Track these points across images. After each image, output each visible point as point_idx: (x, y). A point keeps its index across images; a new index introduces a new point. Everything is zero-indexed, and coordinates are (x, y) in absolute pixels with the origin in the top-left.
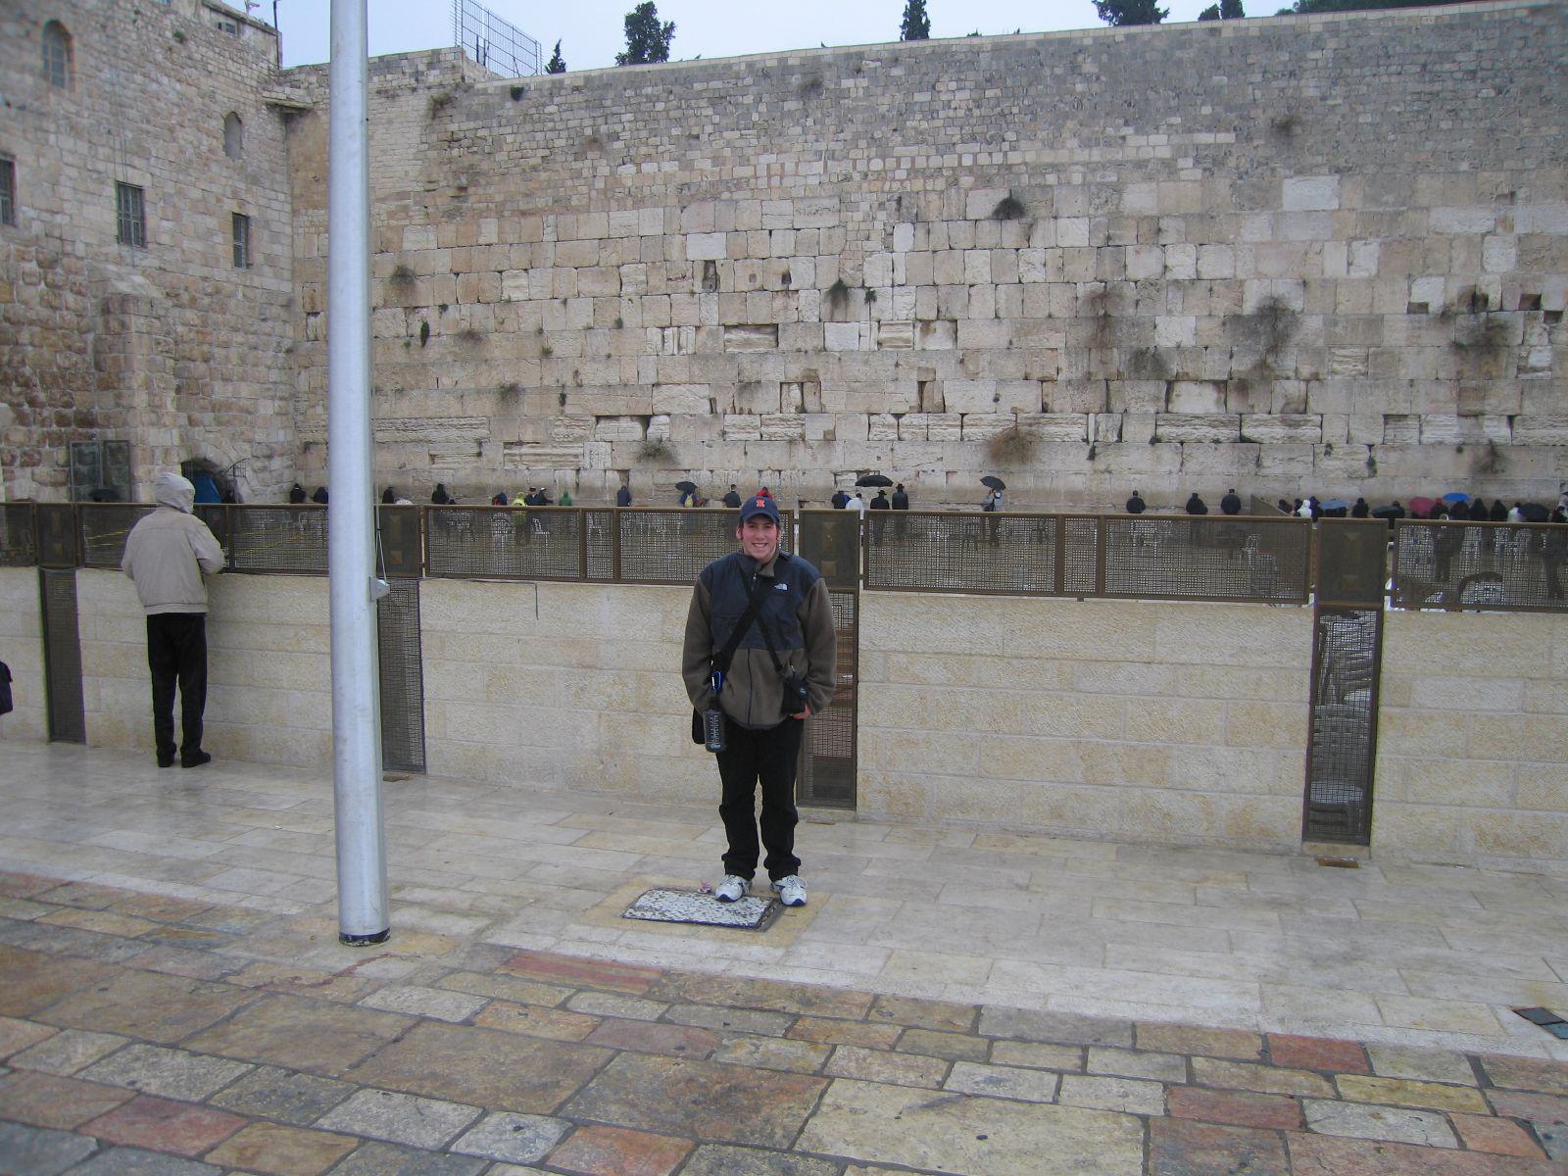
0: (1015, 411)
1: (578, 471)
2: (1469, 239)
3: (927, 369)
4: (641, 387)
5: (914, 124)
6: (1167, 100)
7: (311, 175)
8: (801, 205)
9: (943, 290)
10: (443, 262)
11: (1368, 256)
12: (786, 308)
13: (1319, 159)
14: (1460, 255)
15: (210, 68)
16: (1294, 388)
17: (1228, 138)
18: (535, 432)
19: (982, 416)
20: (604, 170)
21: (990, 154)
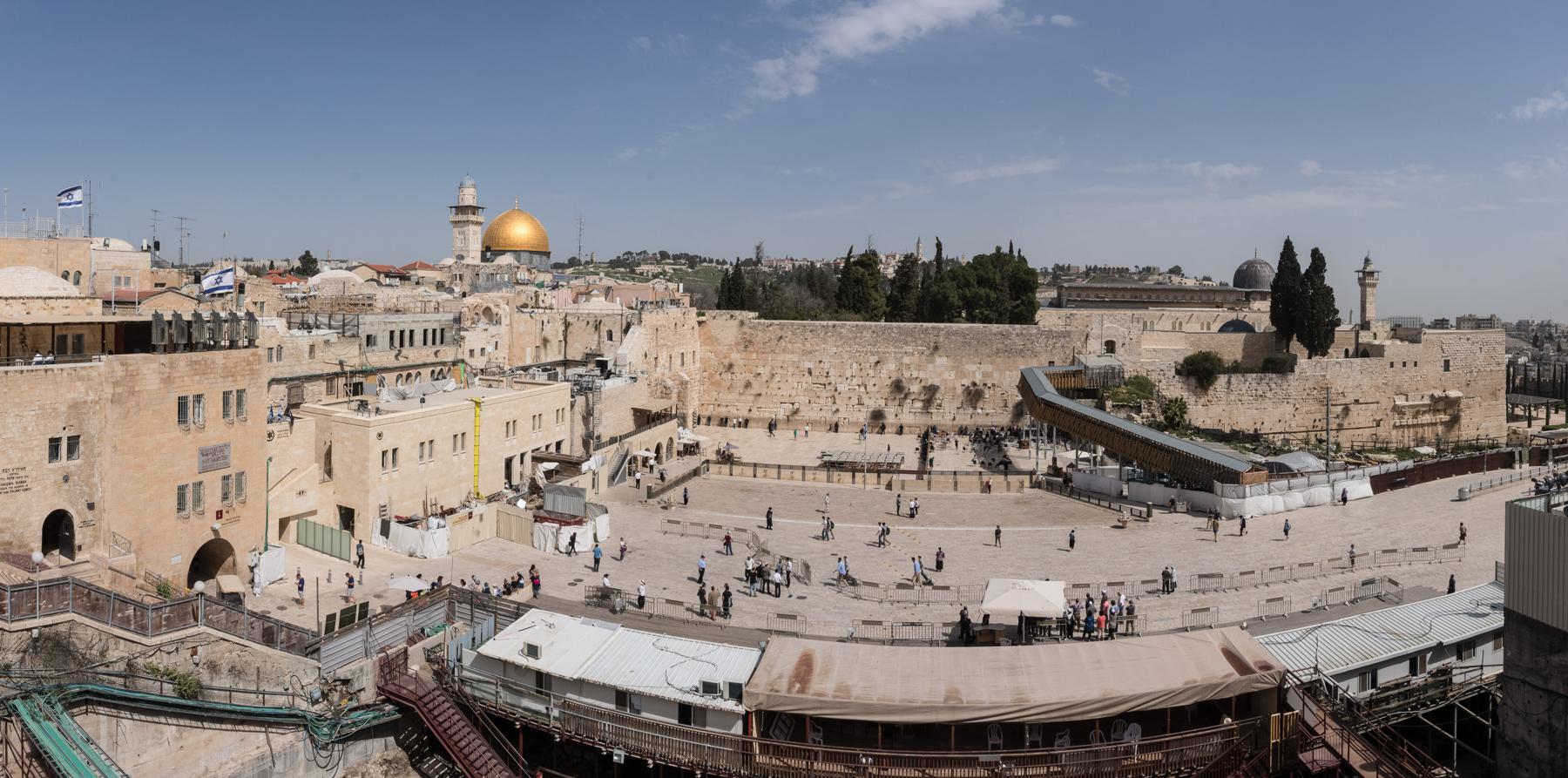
10: (742, 362)
16: (939, 401)
20: (784, 344)
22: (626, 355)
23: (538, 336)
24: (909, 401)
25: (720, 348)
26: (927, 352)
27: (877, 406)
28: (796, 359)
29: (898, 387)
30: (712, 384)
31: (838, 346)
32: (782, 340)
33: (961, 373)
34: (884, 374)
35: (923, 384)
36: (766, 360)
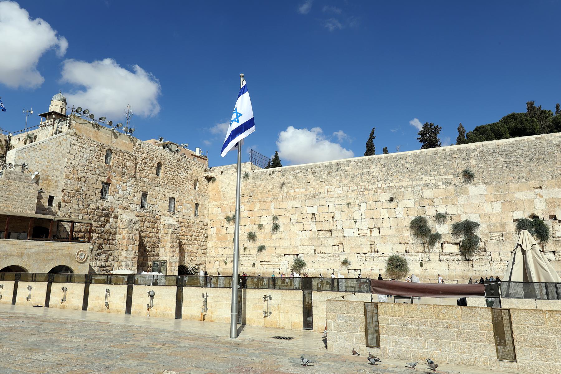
0: (398, 252)
1: (279, 269)
2: (529, 201)
3: (372, 241)
4: (296, 247)
5: (365, 177)
6: (433, 168)
7: (214, 193)
8: (336, 199)
9: (375, 220)
11: (498, 207)
12: (333, 225)
13: (479, 181)
14: (527, 205)
15: (192, 169)
17: (452, 176)
18: (268, 258)
19: (388, 254)
20: (286, 191)
21: (385, 184)
25: (227, 202)
26: (456, 181)
27: (395, 253)
30: (219, 239)
31: (342, 187)
33: (509, 205)
34: (400, 212)
35: (455, 221)
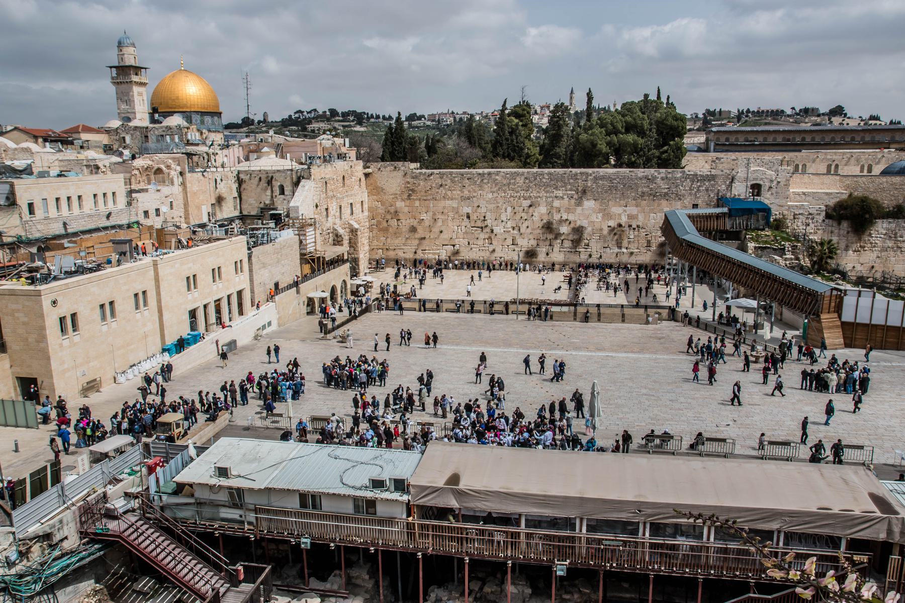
10: (406, 210)
14: (617, 217)
16: (586, 241)
22: (298, 207)
23: (213, 194)
24: (559, 241)
26: (576, 196)
27: (530, 246)
28: (455, 205)
29: (548, 227)
30: (380, 230)
31: (493, 192)
32: (441, 188)
33: (608, 216)
34: (536, 218)
35: (572, 225)
36: (428, 207)
